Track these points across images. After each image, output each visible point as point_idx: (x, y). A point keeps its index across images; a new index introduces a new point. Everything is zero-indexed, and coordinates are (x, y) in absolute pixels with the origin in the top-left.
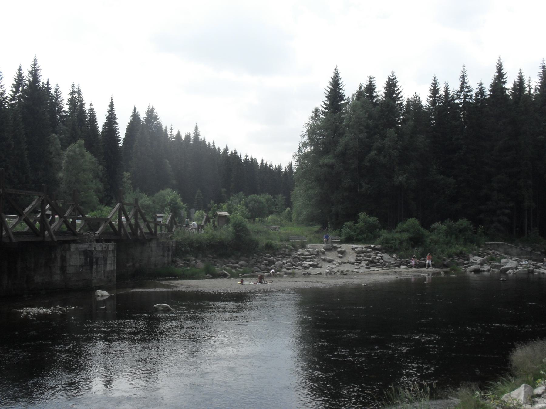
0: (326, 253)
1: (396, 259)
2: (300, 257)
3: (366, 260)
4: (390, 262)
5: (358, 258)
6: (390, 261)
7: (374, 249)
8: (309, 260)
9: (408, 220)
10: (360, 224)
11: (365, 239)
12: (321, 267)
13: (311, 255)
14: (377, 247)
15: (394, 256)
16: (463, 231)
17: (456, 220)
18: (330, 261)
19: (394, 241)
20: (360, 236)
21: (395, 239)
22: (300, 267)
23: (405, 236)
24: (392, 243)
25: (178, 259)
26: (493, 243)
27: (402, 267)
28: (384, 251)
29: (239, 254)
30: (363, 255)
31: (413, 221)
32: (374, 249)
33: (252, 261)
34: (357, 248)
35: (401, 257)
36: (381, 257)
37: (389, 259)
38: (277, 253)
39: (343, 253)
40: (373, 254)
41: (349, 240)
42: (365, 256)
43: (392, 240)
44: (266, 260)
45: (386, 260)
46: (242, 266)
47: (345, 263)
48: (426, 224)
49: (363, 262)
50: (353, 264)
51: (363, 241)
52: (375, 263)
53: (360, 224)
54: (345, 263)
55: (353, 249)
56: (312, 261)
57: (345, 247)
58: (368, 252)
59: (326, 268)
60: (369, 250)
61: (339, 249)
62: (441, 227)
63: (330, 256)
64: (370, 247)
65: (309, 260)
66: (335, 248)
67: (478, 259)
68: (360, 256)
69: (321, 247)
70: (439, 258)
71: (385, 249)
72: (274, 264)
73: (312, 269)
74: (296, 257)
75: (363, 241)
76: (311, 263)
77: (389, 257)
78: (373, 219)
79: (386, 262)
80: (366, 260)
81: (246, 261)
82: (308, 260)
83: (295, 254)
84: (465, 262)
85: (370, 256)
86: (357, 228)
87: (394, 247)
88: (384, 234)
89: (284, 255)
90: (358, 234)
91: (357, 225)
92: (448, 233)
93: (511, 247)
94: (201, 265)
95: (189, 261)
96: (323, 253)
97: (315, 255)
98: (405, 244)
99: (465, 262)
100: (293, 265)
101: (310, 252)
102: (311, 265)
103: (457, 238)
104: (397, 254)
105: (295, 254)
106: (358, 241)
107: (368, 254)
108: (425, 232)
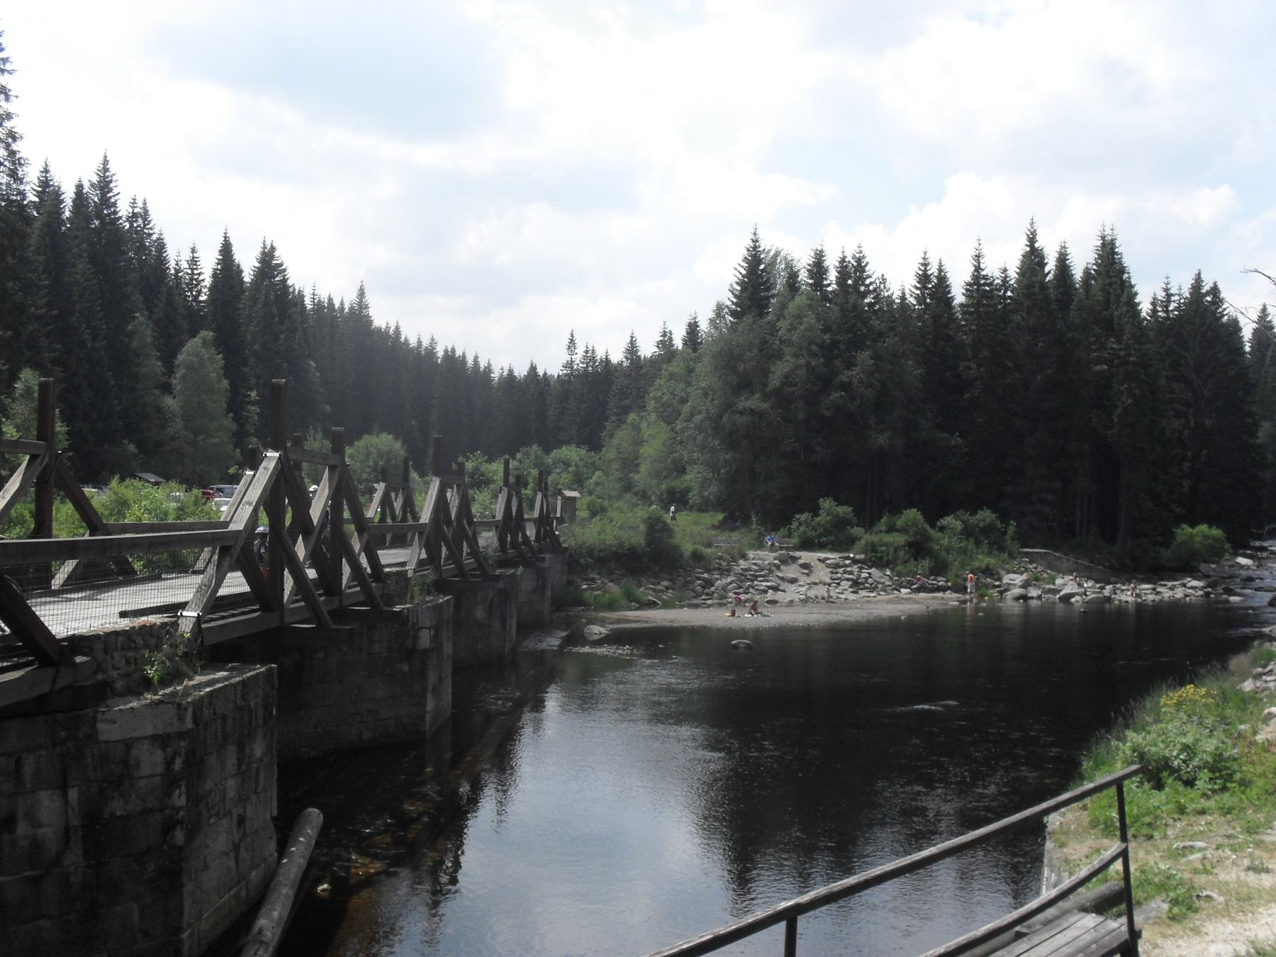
0: (782, 567)
1: (891, 579)
2: (747, 573)
3: (848, 580)
4: (883, 583)
5: (835, 576)
6: (883, 580)
7: (855, 561)
10: (823, 518)
11: (832, 543)
12: (784, 591)
13: (762, 570)
14: (857, 557)
15: (888, 573)
16: (987, 530)
17: (974, 513)
18: (793, 581)
19: (884, 548)
20: (824, 539)
21: (886, 544)
22: (751, 590)
23: (899, 539)
24: (881, 552)
25: (575, 578)
26: (1031, 550)
27: (903, 590)
28: (870, 564)
29: (657, 569)
30: (841, 570)
32: (855, 561)
33: (680, 581)
34: (829, 559)
35: (899, 574)
36: (869, 573)
37: (881, 577)
39: (806, 566)
40: (855, 568)
42: (845, 572)
43: (881, 546)
44: (699, 579)
45: (877, 580)
47: (816, 584)
48: (932, 519)
49: (843, 583)
51: (830, 546)
52: (862, 584)
53: (823, 518)
55: (822, 561)
56: (767, 581)
57: (806, 556)
58: (846, 566)
59: (792, 593)
60: (847, 562)
61: (801, 561)
62: (952, 522)
63: (790, 571)
64: (848, 558)
66: (794, 559)
67: (1019, 579)
68: (837, 573)
69: (768, 557)
72: (713, 585)
74: (742, 575)
75: (830, 546)
76: (769, 584)
77: (881, 574)
78: (844, 510)
79: (879, 583)
80: (848, 580)
81: (670, 580)
82: (759, 579)
83: (737, 569)
85: (850, 573)
86: (819, 525)
87: (885, 559)
88: (865, 537)
89: (725, 572)
90: (819, 536)
91: (817, 519)
92: (968, 532)
93: (1059, 558)
94: (614, 589)
95: (593, 580)
96: (778, 567)
98: (902, 553)
99: (997, 583)
100: (740, 587)
101: (759, 566)
102: (770, 588)
103: (978, 543)
104: (892, 570)
105: (737, 569)
106: (821, 547)
107: (849, 569)
108: (932, 532)
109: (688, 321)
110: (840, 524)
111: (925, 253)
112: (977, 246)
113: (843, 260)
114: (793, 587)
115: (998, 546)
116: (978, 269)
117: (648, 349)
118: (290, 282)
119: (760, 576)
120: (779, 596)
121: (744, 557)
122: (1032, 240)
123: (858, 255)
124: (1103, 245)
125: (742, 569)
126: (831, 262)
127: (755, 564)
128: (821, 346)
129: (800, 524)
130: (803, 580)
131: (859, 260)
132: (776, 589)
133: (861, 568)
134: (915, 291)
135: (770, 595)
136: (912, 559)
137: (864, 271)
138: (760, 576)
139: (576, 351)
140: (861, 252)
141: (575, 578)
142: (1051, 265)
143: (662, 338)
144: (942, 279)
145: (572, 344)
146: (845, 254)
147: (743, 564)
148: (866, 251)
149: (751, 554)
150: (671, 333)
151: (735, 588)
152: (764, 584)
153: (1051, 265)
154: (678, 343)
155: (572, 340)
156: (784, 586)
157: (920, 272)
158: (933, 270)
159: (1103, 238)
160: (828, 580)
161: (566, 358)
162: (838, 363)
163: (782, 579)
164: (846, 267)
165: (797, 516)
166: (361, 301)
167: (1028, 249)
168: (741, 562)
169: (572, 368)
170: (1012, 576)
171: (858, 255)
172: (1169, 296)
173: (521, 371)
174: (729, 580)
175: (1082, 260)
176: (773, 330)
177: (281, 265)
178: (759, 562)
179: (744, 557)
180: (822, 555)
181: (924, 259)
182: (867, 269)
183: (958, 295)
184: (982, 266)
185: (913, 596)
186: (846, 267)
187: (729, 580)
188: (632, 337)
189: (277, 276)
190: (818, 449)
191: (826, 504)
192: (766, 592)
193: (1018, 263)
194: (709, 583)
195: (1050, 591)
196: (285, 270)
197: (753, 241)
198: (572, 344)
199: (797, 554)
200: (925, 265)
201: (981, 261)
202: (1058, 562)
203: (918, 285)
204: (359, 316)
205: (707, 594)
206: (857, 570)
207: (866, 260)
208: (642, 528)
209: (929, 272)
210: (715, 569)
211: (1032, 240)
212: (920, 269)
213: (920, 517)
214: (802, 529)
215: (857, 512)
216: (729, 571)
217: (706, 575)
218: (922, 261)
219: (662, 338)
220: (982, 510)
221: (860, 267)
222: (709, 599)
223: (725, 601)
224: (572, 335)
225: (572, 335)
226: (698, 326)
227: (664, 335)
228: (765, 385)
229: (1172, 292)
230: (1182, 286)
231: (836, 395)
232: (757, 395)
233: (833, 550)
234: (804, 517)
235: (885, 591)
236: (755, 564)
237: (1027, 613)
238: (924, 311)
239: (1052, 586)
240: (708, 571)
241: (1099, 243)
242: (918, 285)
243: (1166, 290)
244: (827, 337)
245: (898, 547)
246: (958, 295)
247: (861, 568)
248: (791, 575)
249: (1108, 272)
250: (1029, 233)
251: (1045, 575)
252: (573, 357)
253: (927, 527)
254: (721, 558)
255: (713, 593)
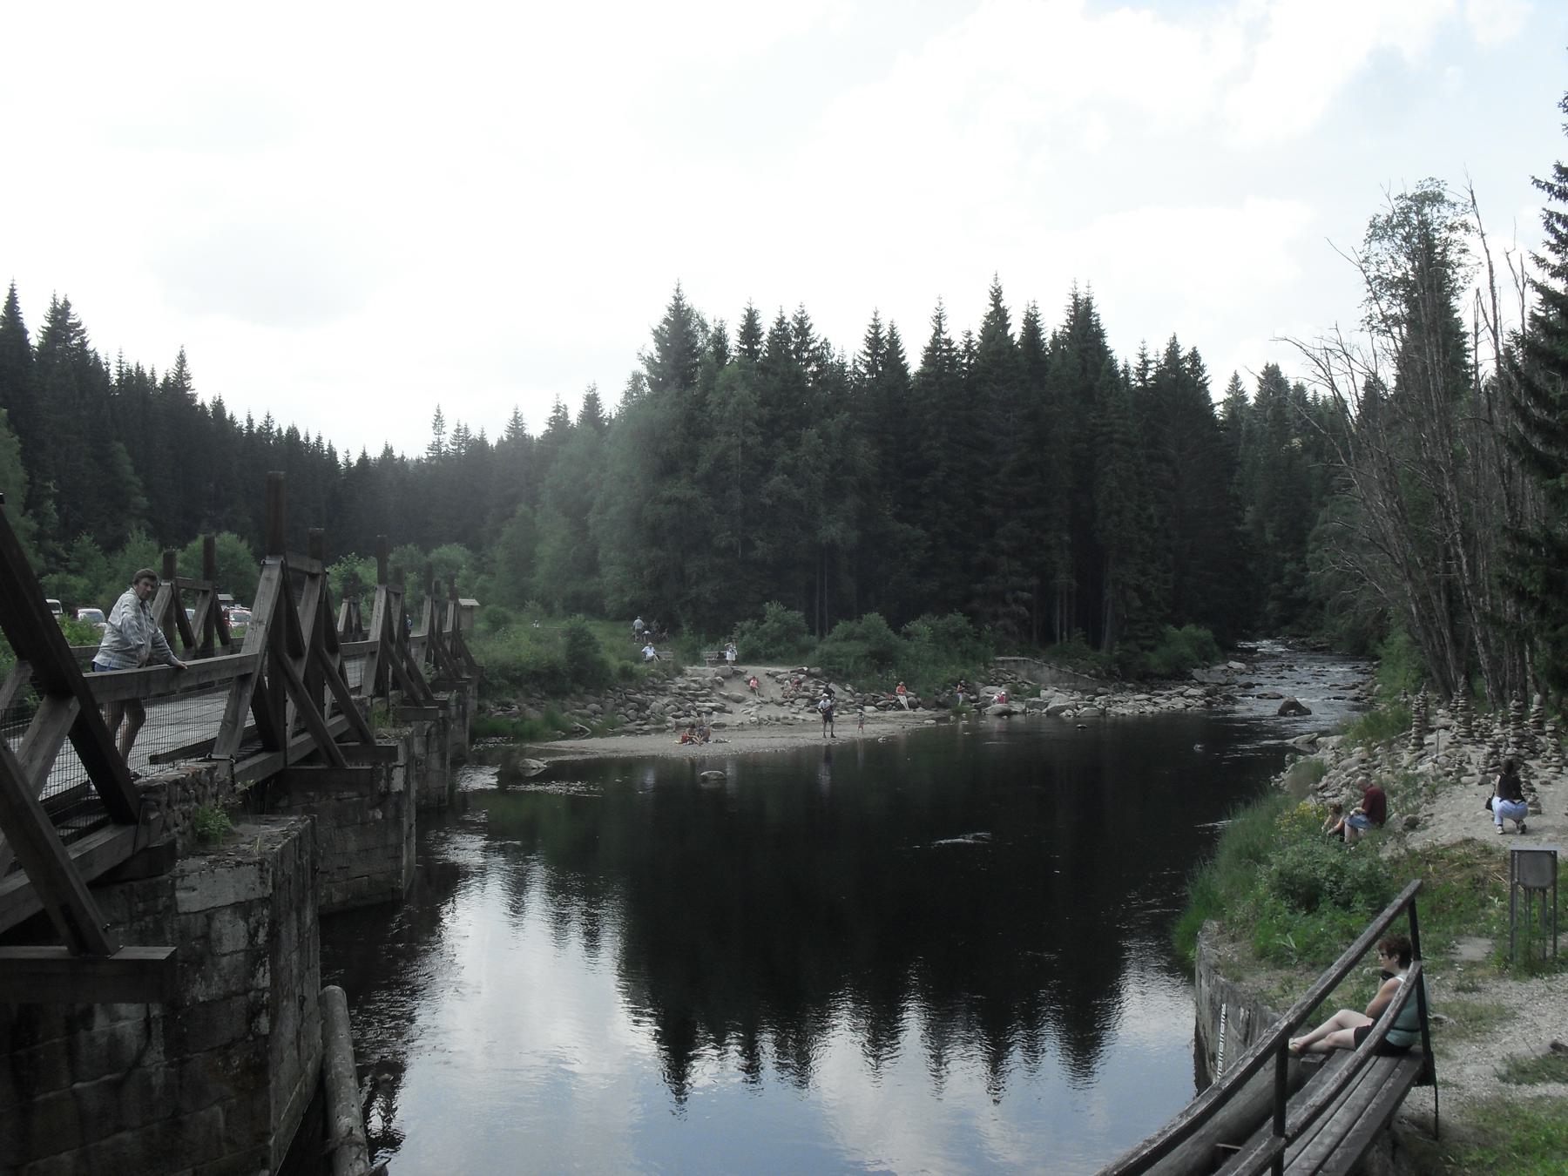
0: (725, 684)
1: (853, 695)
2: (686, 692)
3: (803, 697)
4: (844, 701)
6: (843, 697)
8: (704, 699)
9: (865, 616)
11: (781, 654)
12: (730, 712)
13: (702, 689)
14: (812, 670)
15: (849, 688)
16: (957, 636)
18: (739, 701)
20: (772, 650)
22: (693, 712)
23: (859, 648)
24: (840, 663)
29: (582, 690)
31: (874, 619)
32: (810, 675)
34: (780, 673)
37: (842, 693)
38: (643, 687)
41: (749, 657)
46: (595, 712)
48: (896, 623)
49: (797, 701)
50: (781, 704)
54: (767, 703)
57: (755, 671)
59: (739, 715)
62: (921, 626)
63: (735, 689)
64: (801, 672)
65: (704, 699)
69: (709, 672)
70: (928, 690)
71: (827, 675)
73: (718, 717)
74: (680, 694)
75: (779, 658)
76: (713, 705)
77: (841, 690)
78: (796, 616)
80: (803, 697)
82: (700, 699)
84: (972, 697)
85: (806, 689)
86: (765, 633)
89: (660, 691)
97: (709, 688)
99: (972, 697)
100: (679, 710)
101: (699, 683)
102: (714, 709)
104: (853, 685)
106: (770, 659)
108: (895, 638)
109: (586, 393)
110: (790, 633)
111: (876, 314)
112: (937, 305)
113: (781, 322)
114: (739, 708)
115: (969, 656)
116: (939, 331)
117: (536, 428)
118: (90, 347)
119: (703, 695)
120: (725, 718)
121: (680, 673)
122: (997, 297)
123: (799, 316)
124: (1076, 305)
125: (680, 688)
126: (767, 325)
127: (694, 681)
128: (759, 423)
129: (743, 634)
130: (752, 699)
131: (801, 322)
132: (721, 710)
133: (817, 683)
134: (864, 357)
135: (716, 718)
136: (875, 671)
137: (808, 335)
138: (703, 695)
139: (444, 430)
140: (803, 312)
141: (488, 703)
142: (1016, 330)
143: (555, 414)
144: (894, 342)
145: (438, 422)
146: (783, 314)
147: (680, 682)
148: (809, 312)
149: (689, 669)
150: (566, 409)
151: (673, 710)
152: (708, 704)
153: (1016, 330)
154: (574, 418)
155: (438, 417)
156: (730, 706)
157: (871, 336)
158: (884, 333)
159: (1075, 297)
160: (780, 699)
161: (431, 438)
162: (780, 442)
163: (726, 698)
164: (785, 329)
165: (739, 624)
166: (181, 370)
167: (992, 309)
168: (678, 679)
169: (440, 450)
170: (990, 688)
171: (799, 316)
172: (1146, 363)
173: (375, 453)
174: (666, 700)
175: (1054, 323)
176: (701, 403)
177: (78, 324)
178: (700, 679)
179: (680, 673)
180: (772, 669)
181: (875, 320)
182: (811, 331)
183: (914, 362)
184: (944, 329)
185: (880, 714)
186: (785, 329)
187: (666, 700)
188: (516, 413)
189: (73, 338)
190: (758, 543)
191: (772, 608)
192: (711, 714)
193: (980, 326)
194: (643, 706)
195: (1034, 705)
196: (83, 331)
197: (676, 299)
198: (438, 422)
199: (742, 668)
200: (876, 327)
201: (943, 323)
202: (1038, 671)
203: (869, 351)
204: (177, 389)
205: (642, 719)
206: (813, 685)
207: (809, 322)
208: (562, 641)
209: (881, 336)
210: (648, 688)
211: (997, 297)
212: (871, 333)
213: (882, 622)
214: (747, 636)
215: (809, 619)
216: (664, 689)
217: (639, 696)
218: (872, 323)
219: (555, 414)
220: (952, 612)
221: (803, 330)
222: (645, 724)
223: (664, 726)
224: (438, 411)
225: (438, 411)
226: (598, 400)
227: (558, 410)
228: (693, 470)
229: (1150, 357)
230: (1157, 351)
231: (776, 481)
232: (683, 481)
233: (782, 663)
234: (748, 624)
235: (846, 709)
236: (694, 681)
237: (1010, 732)
238: (876, 380)
239: (1037, 699)
240: (640, 691)
241: (1071, 302)
242: (869, 351)
243: (1143, 356)
244: (766, 411)
245: (859, 657)
246: (914, 362)
247: (817, 683)
248: (738, 693)
249: (1084, 335)
250: (993, 291)
251: (1026, 687)
252: (441, 437)
253: (890, 632)
254: (654, 675)
255: (649, 717)
